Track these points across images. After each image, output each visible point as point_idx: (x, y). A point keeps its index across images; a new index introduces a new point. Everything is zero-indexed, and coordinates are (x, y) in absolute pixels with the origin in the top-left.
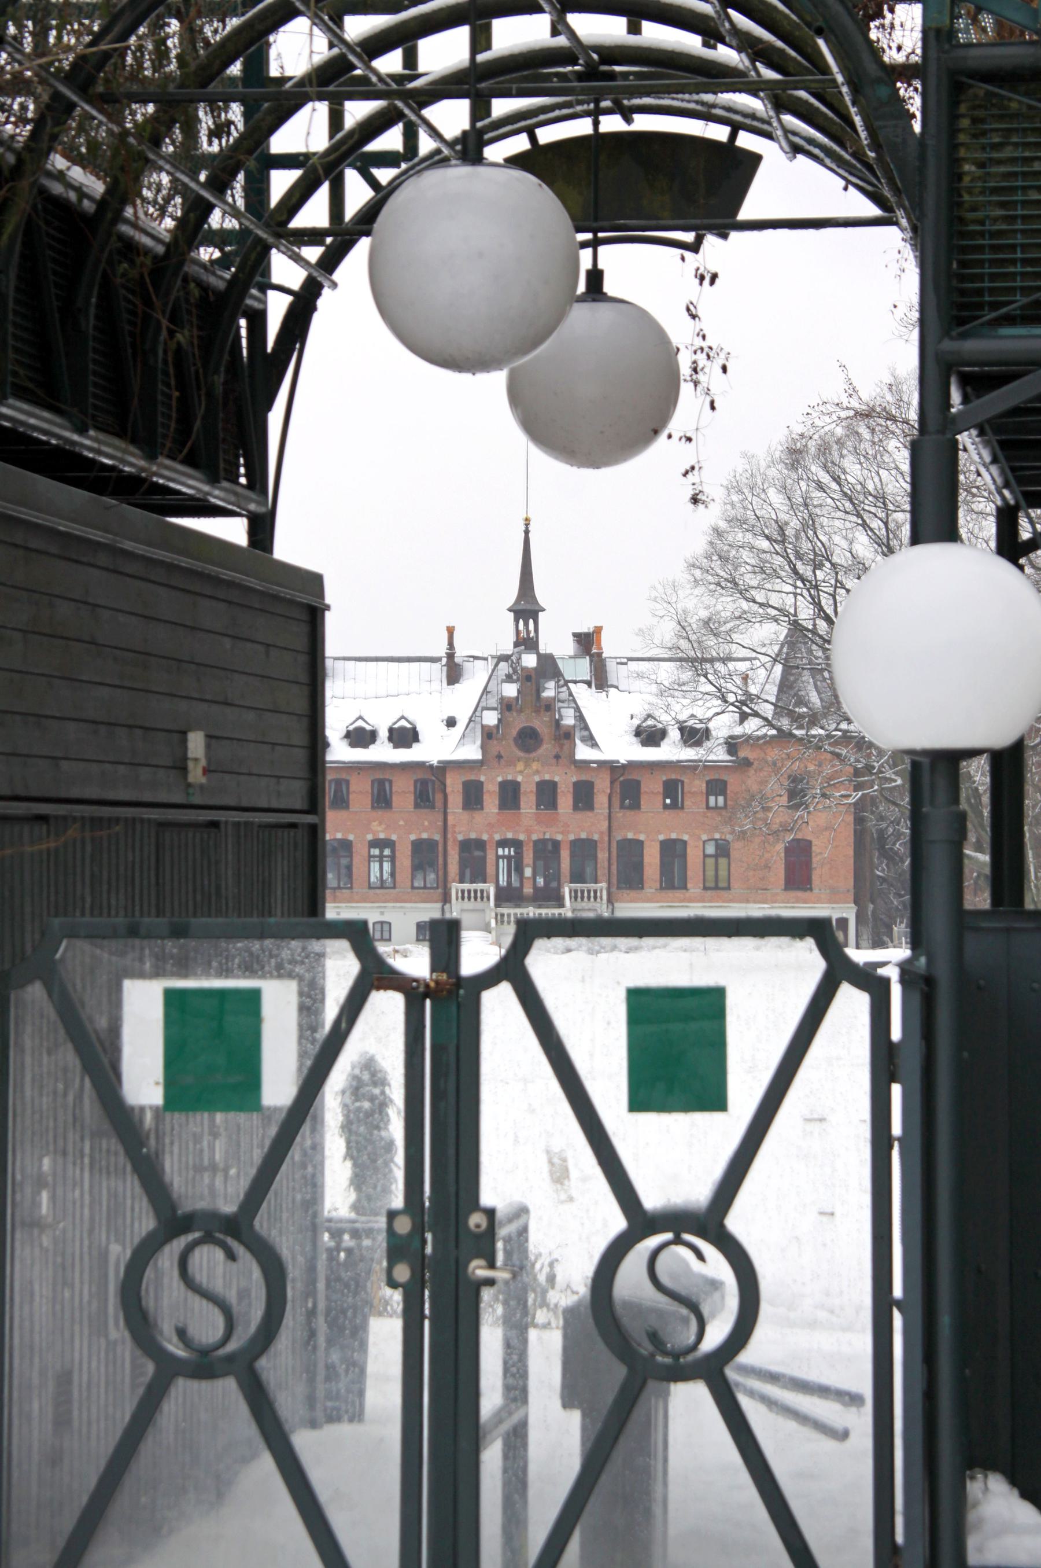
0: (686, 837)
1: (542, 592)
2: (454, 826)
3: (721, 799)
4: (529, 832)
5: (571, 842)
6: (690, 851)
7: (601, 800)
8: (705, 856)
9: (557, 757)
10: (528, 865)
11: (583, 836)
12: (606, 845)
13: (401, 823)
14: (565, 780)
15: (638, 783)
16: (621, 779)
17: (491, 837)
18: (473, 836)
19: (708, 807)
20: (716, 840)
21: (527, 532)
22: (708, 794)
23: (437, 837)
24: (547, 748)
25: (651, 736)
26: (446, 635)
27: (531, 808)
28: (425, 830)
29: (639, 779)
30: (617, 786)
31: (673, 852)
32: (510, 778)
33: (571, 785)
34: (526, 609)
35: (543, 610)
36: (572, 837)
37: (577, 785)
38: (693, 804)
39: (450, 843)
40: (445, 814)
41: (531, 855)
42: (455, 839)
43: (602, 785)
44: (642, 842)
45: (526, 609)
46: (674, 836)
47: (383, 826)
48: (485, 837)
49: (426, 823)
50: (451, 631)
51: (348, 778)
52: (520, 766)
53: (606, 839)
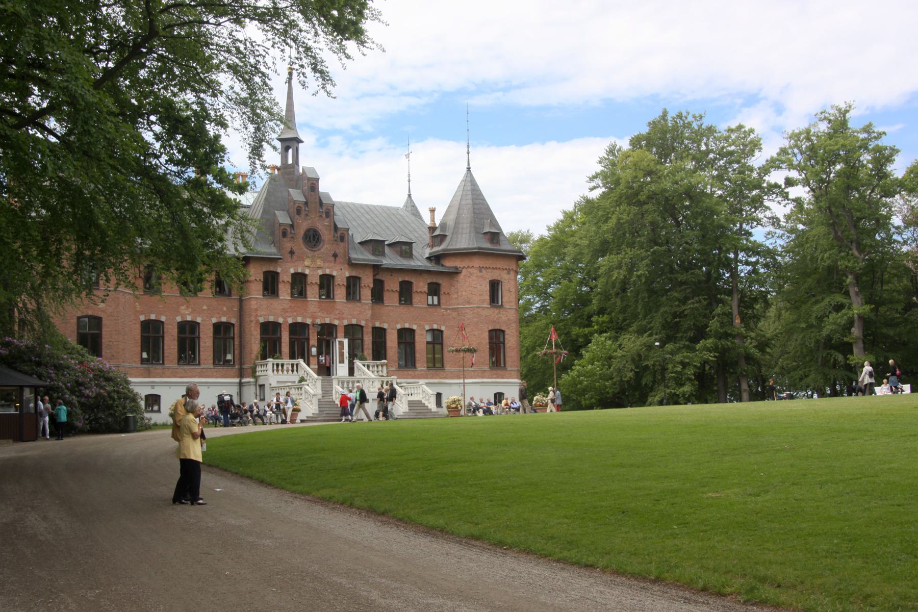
0: (415, 327)
2: (256, 310)
3: (436, 298)
4: (313, 317)
6: (417, 338)
10: (313, 346)
11: (354, 322)
13: (205, 307)
14: (341, 274)
17: (285, 321)
18: (271, 319)
24: (326, 247)
27: (315, 297)
28: (224, 315)
29: (383, 279)
32: (300, 271)
33: (345, 280)
35: (302, 142)
36: (346, 323)
37: (348, 278)
38: (419, 300)
42: (257, 321)
44: (385, 330)
46: (407, 326)
47: (190, 310)
48: (281, 320)
49: (225, 309)
52: (307, 262)
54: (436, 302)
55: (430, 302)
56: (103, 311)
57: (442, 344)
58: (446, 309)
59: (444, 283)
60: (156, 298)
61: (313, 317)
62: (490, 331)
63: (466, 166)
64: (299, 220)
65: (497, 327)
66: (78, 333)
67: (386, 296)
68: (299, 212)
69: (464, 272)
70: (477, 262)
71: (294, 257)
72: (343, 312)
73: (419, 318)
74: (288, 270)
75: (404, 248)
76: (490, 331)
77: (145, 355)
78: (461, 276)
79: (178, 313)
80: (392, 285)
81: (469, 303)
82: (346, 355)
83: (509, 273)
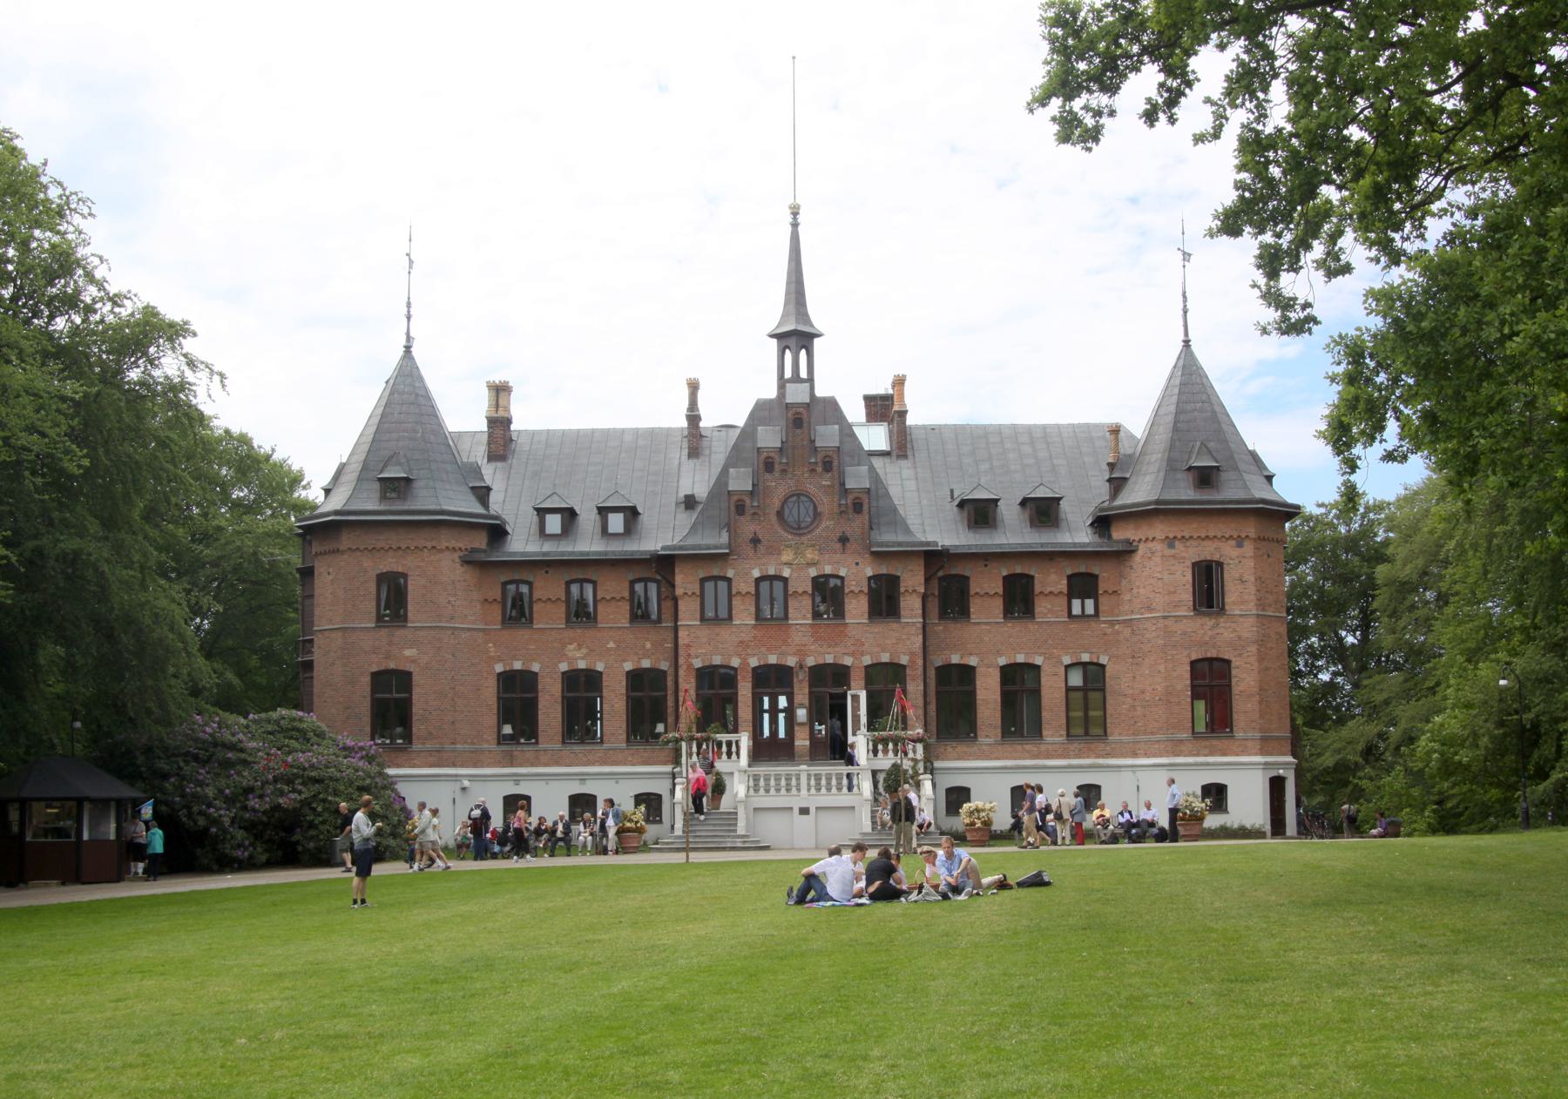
0: (1038, 661)
1: (819, 315)
2: (689, 646)
3: (1090, 603)
4: (802, 653)
5: (867, 667)
7: (911, 606)
8: (1069, 689)
9: (844, 540)
10: (801, 706)
11: (885, 658)
12: (920, 671)
13: (611, 645)
15: (967, 579)
16: (940, 574)
17: (745, 663)
18: (717, 660)
19: (1070, 615)
20: (1084, 665)
21: (795, 225)
22: (1070, 596)
23: (664, 666)
25: (980, 513)
26: (686, 392)
27: (804, 617)
28: (645, 656)
29: (967, 573)
30: (935, 584)
31: (1019, 683)
34: (797, 338)
36: (867, 660)
38: (1048, 609)
39: (681, 672)
40: (676, 629)
41: (806, 691)
42: (690, 666)
43: (913, 580)
44: (973, 668)
45: (797, 338)
46: (1020, 659)
47: (584, 651)
49: (648, 645)
50: (694, 387)
51: (531, 579)
52: (787, 556)
53: (920, 662)
54: (1090, 609)
55: (1076, 610)
56: (413, 661)
57: (1103, 690)
58: (1112, 623)
59: (1105, 574)
60: (522, 634)
61: (802, 653)
62: (1193, 663)
63: (1182, 337)
64: (771, 481)
65: (1212, 653)
66: (374, 700)
67: (975, 606)
68: (769, 466)
69: (1142, 549)
70: (1160, 529)
71: (761, 548)
72: (863, 642)
73: (1050, 645)
74: (748, 573)
75: (1043, 511)
76: (1193, 663)
77: (508, 729)
78: (1137, 558)
79: (562, 656)
80: (987, 585)
81: (1150, 609)
82: (864, 720)
83: (1240, 545)
